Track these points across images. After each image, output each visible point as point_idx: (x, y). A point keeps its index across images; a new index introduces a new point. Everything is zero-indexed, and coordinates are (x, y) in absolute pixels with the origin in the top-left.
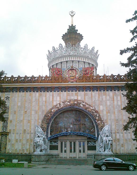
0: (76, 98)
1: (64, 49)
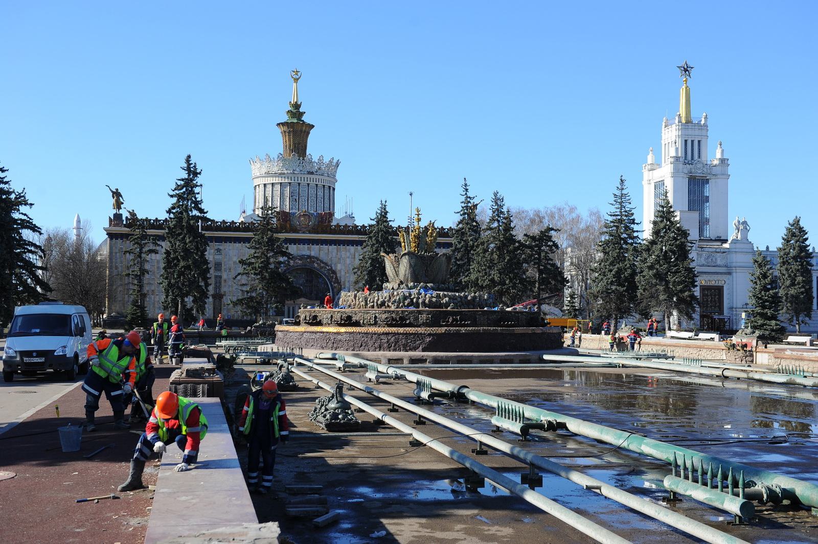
0: (308, 254)
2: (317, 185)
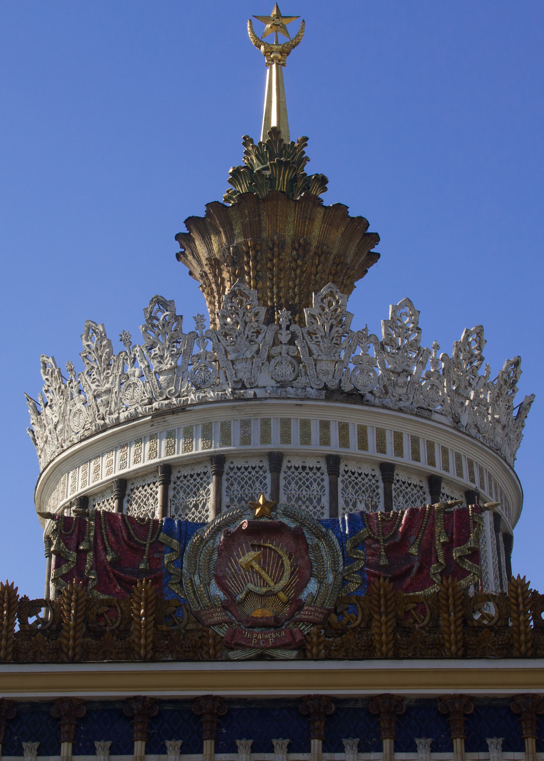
1: (197, 350)
2: (387, 470)
